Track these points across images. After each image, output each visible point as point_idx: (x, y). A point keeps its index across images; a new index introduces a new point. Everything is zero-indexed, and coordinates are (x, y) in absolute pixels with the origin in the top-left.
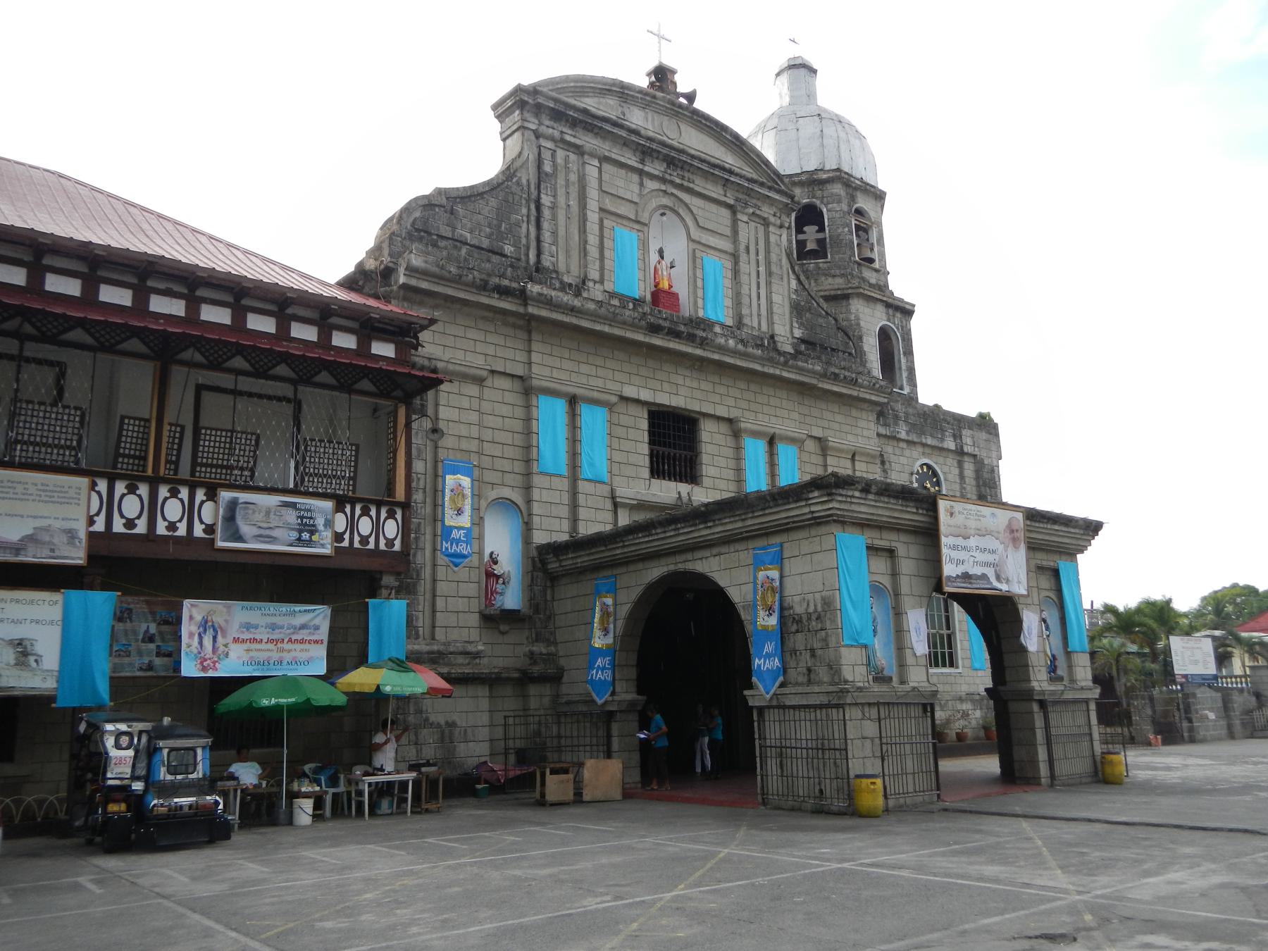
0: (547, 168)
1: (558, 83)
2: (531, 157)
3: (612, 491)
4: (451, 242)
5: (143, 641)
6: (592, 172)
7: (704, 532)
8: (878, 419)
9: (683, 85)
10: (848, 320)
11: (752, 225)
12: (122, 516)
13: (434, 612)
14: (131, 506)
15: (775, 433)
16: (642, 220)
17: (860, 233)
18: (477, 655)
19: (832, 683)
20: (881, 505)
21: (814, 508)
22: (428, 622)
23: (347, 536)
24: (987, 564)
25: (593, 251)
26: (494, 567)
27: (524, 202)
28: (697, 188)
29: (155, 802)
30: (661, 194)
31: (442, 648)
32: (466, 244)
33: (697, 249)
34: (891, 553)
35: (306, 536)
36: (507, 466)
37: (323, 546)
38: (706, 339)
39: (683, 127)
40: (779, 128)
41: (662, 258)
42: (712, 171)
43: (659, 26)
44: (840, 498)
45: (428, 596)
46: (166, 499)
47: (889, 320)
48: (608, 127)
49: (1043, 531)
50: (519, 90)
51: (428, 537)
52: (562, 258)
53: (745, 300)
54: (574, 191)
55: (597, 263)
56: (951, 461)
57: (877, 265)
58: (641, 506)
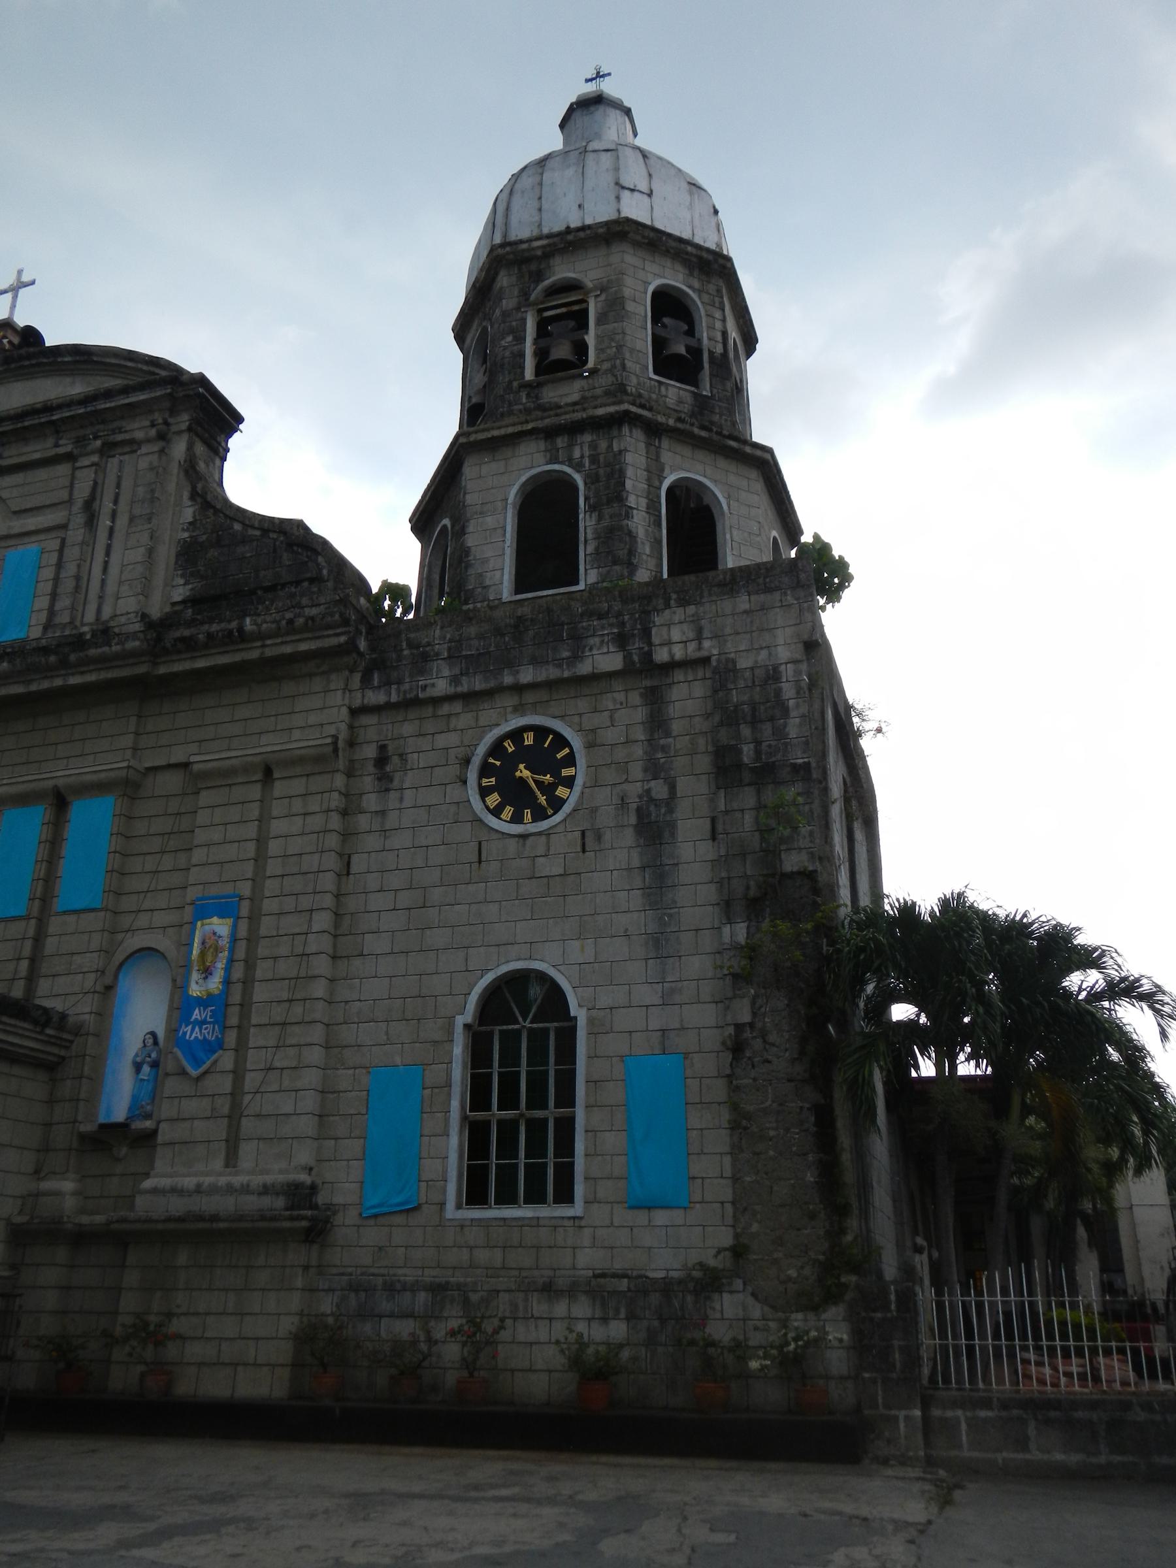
15: (56, 786)
42: (20, 425)
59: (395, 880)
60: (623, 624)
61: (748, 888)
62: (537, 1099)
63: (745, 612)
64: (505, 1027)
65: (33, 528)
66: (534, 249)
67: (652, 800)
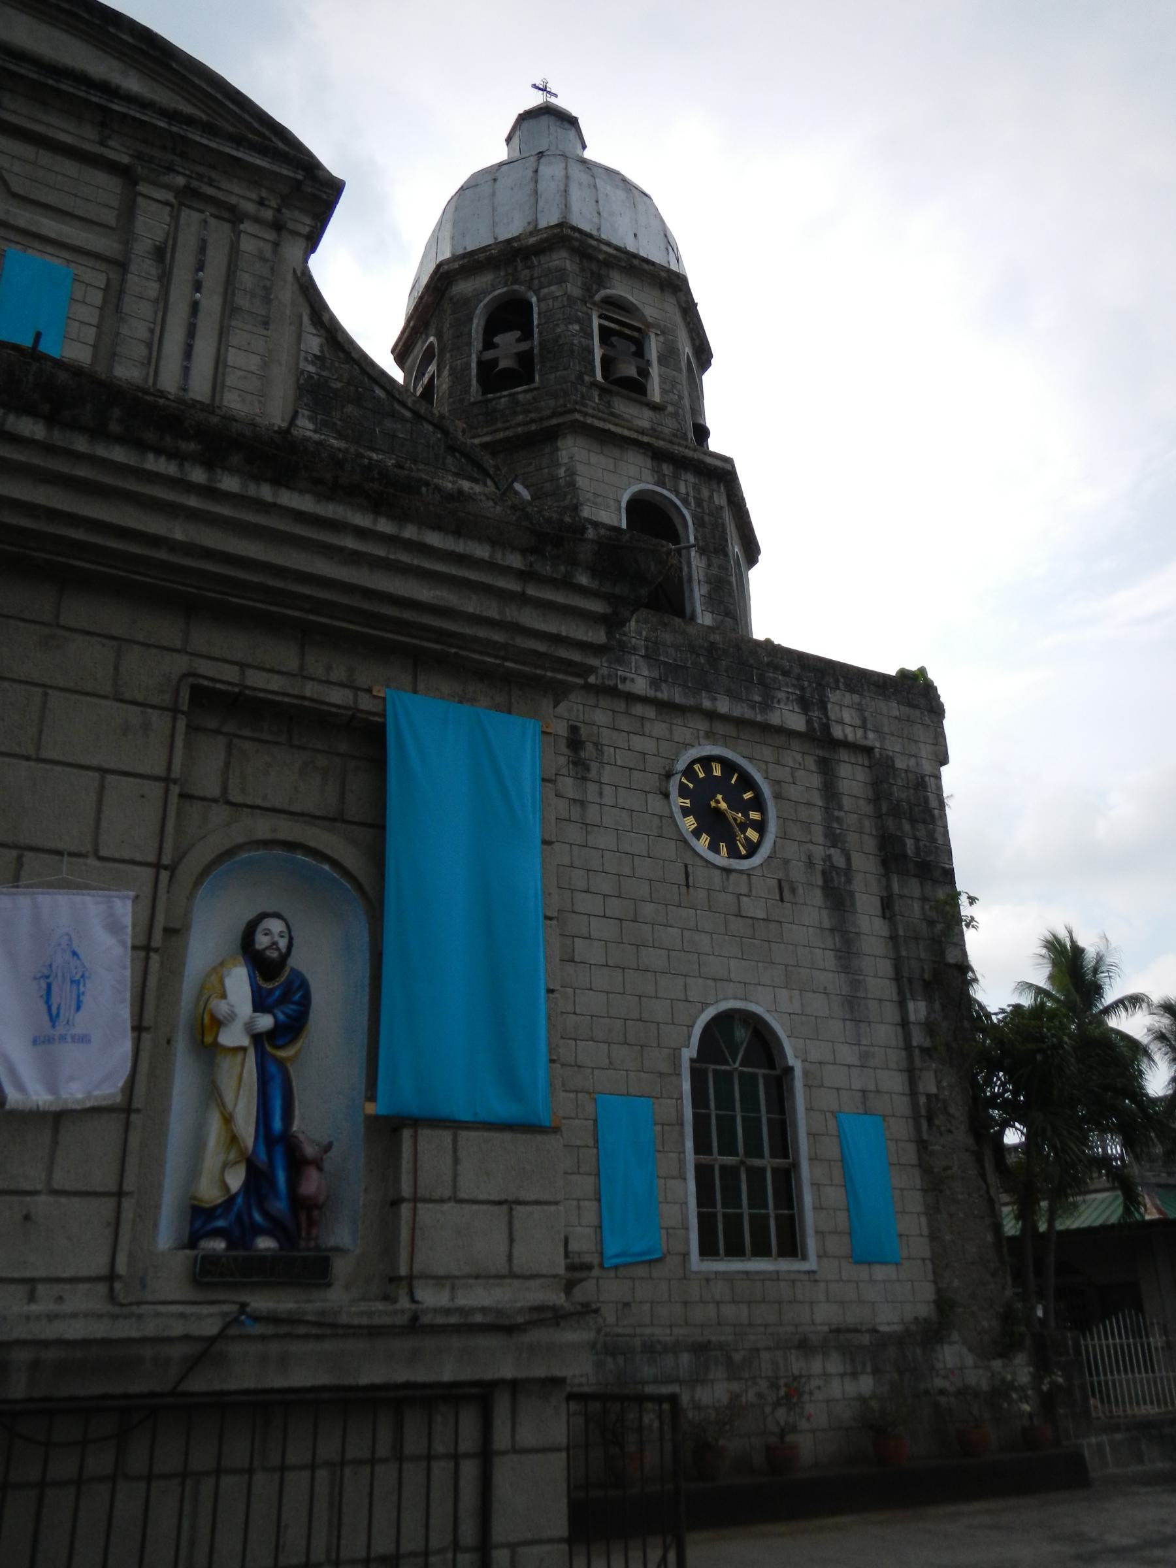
10: (553, 479)
47: (657, 484)
49: (193, 502)
59: (603, 885)
60: (802, 689)
61: (923, 970)
62: (754, 1149)
63: (896, 718)
64: (718, 1067)
65: (53, 235)
66: (601, 251)
67: (833, 866)
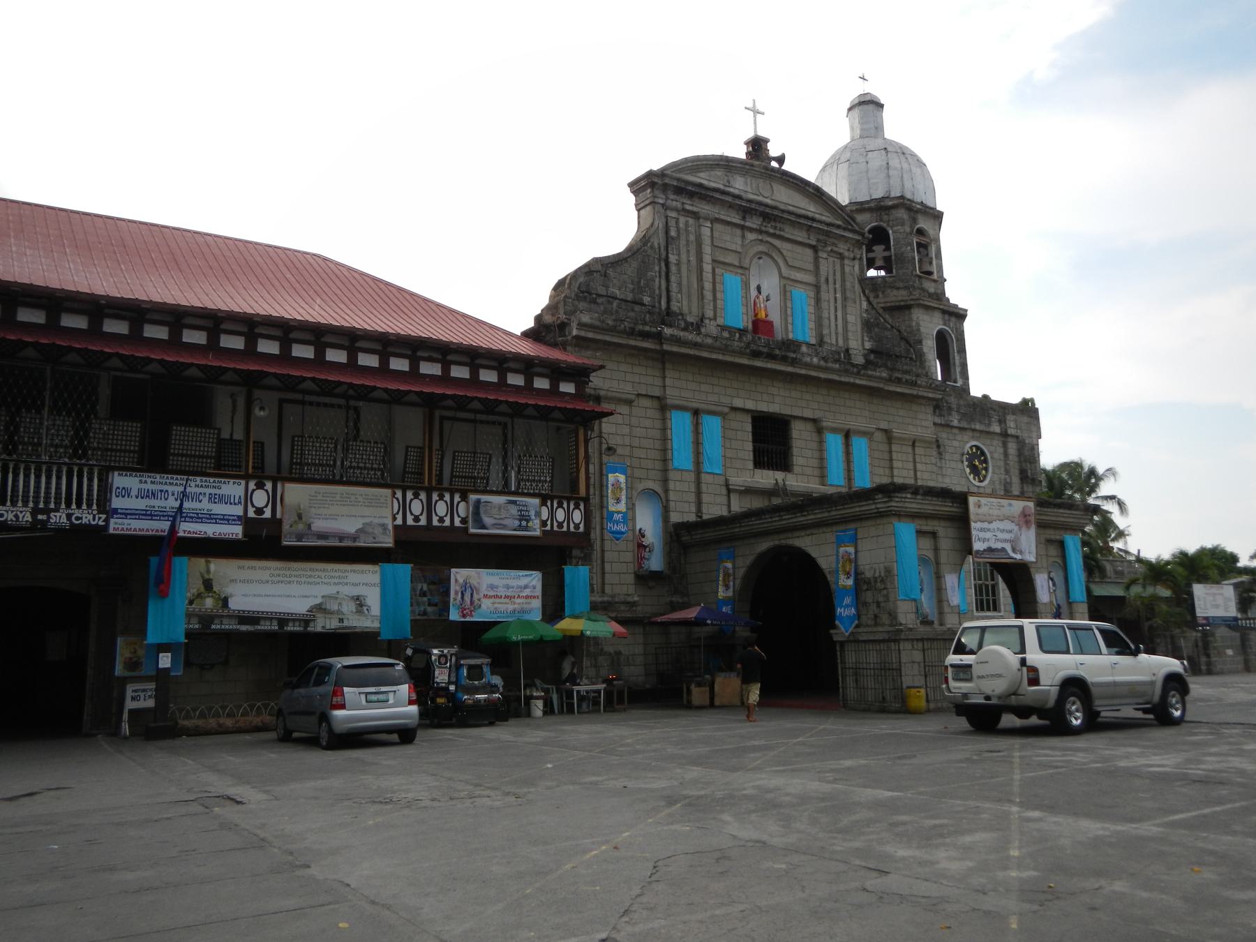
0: (673, 233)
1: (679, 165)
2: (660, 225)
3: (727, 480)
4: (605, 298)
5: (420, 596)
6: (706, 232)
7: (801, 519)
8: (934, 411)
9: (774, 150)
10: (910, 326)
11: (831, 259)
12: (412, 514)
13: (603, 573)
14: (417, 507)
16: (744, 266)
17: (921, 249)
18: (634, 604)
19: (891, 625)
20: (927, 502)
21: (879, 506)
22: (600, 580)
23: (549, 523)
24: (1005, 541)
25: (708, 295)
26: (643, 539)
27: (656, 261)
28: (787, 236)
29: (466, 697)
30: (758, 242)
31: (610, 599)
32: (616, 298)
33: (787, 284)
34: (934, 535)
35: (524, 523)
36: (650, 464)
37: (535, 530)
38: (796, 358)
39: (776, 186)
40: (851, 161)
41: (760, 293)
43: (754, 101)
44: (897, 499)
45: (599, 562)
46: (436, 501)
47: (945, 325)
48: (717, 195)
50: (650, 174)
51: (598, 519)
52: (683, 304)
53: (826, 322)
54: (693, 248)
55: (712, 304)
56: (997, 442)
57: (935, 276)
58: (748, 491)
65: (799, 279)
67: (1007, 482)
